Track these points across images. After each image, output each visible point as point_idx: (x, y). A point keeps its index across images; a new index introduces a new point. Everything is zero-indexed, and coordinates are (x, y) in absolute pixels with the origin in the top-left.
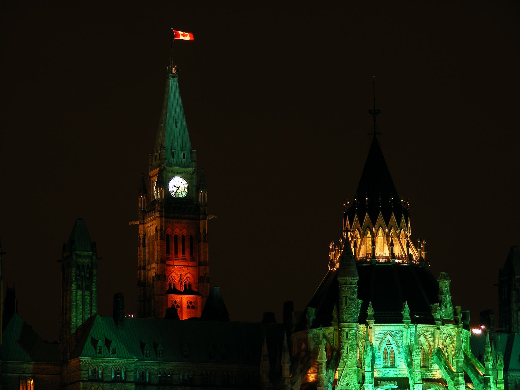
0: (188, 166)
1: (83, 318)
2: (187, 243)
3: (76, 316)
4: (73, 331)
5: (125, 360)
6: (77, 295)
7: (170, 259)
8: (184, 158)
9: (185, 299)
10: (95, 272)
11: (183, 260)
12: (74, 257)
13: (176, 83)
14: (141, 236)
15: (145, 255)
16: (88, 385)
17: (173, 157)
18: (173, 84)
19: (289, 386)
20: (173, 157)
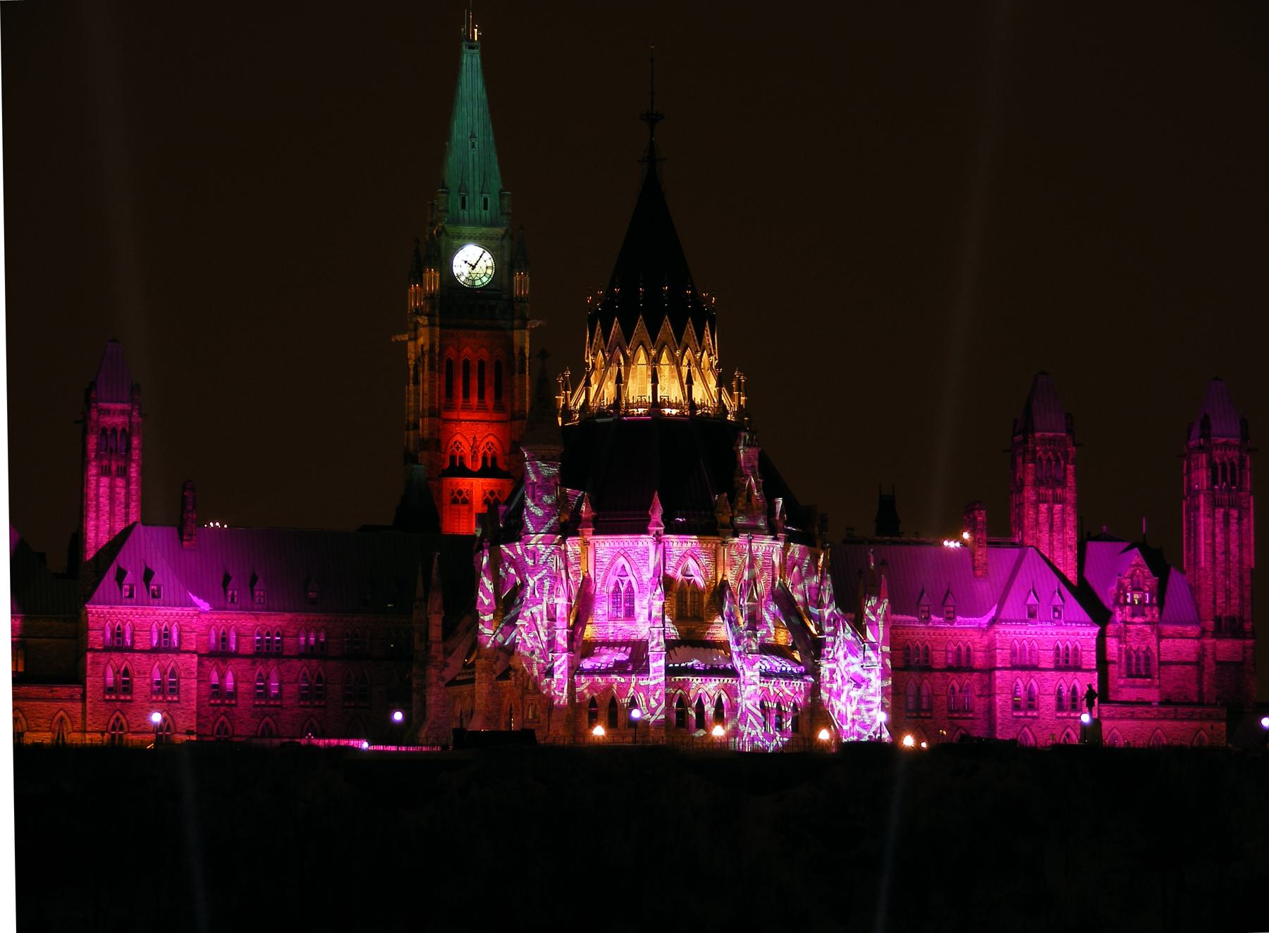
0: (492, 224)
1: (111, 530)
2: (490, 376)
3: (97, 527)
4: (90, 555)
5: (177, 610)
6: (99, 487)
7: (450, 407)
8: (486, 208)
9: (477, 487)
10: (135, 442)
11: (479, 409)
12: (94, 415)
13: (477, 60)
14: (411, 363)
15: (417, 401)
16: (103, 658)
17: (463, 207)
18: (471, 61)
19: (441, 658)
20: (463, 207)
